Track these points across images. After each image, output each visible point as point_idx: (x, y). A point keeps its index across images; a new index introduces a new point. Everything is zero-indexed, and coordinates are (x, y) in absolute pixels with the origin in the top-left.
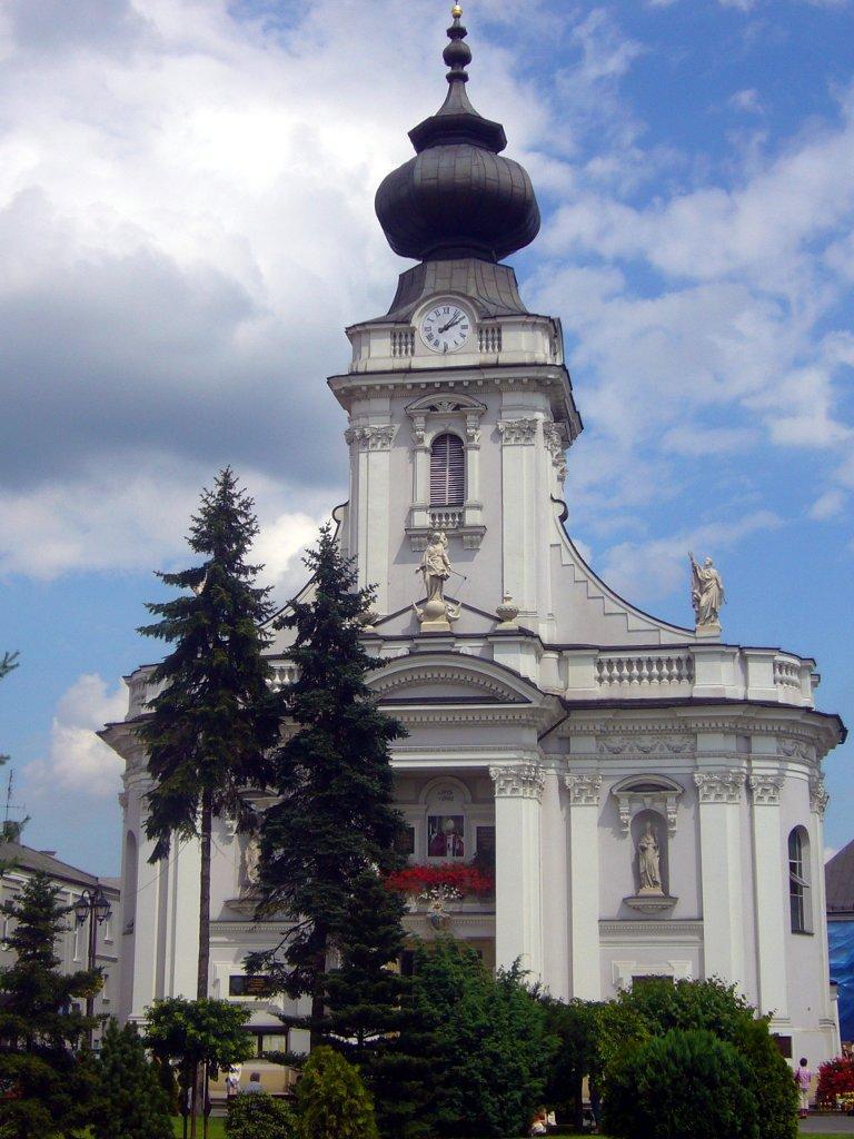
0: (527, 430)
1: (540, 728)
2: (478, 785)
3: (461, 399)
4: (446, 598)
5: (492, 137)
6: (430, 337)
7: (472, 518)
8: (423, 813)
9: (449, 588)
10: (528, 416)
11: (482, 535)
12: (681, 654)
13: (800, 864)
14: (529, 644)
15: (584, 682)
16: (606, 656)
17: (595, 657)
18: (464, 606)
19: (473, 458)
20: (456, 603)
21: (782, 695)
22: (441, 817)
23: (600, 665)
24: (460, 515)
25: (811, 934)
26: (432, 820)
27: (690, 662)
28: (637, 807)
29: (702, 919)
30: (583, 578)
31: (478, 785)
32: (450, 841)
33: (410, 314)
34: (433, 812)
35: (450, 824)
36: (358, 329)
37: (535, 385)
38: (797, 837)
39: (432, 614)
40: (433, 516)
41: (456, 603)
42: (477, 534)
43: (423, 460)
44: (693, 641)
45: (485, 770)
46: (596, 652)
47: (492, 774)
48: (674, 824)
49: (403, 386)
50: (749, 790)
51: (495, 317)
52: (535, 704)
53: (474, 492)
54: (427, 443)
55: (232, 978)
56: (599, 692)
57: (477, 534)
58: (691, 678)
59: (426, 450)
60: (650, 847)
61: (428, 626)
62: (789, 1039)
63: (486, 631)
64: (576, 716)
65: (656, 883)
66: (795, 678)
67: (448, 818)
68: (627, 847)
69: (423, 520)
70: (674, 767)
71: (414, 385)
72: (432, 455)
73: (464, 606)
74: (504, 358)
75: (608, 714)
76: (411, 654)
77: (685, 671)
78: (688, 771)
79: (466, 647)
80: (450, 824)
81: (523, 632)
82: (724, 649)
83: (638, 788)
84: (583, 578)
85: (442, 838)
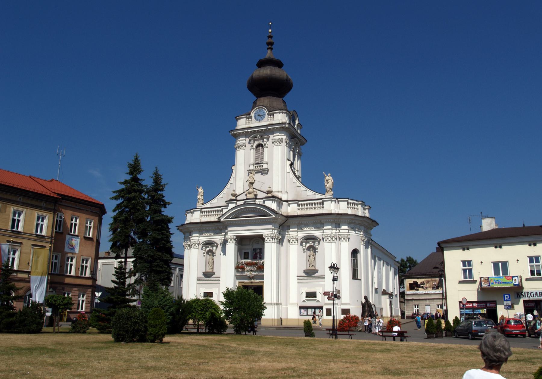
0: (280, 141)
1: (280, 223)
2: (260, 239)
3: (262, 134)
4: (254, 188)
5: (278, 64)
6: (255, 118)
7: (265, 166)
8: (251, 248)
9: (255, 186)
10: (280, 137)
11: (268, 171)
12: (321, 201)
13: (357, 260)
14: (275, 201)
15: (292, 210)
16: (300, 203)
17: (297, 203)
18: (258, 190)
19: (266, 150)
20: (256, 189)
21: (350, 212)
22: (256, 249)
23: (299, 205)
24: (263, 166)
25: (360, 280)
26: (254, 249)
27: (323, 204)
28: (308, 245)
29: (324, 276)
30: (296, 181)
31: (260, 239)
32: (258, 255)
33: (251, 113)
34: (254, 248)
35: (258, 251)
36: (238, 118)
37: (282, 129)
38: (355, 252)
39: (250, 193)
40: (256, 167)
41: (256, 189)
42: (266, 171)
43: (253, 152)
44: (324, 197)
45: (262, 235)
46: (297, 202)
47: (264, 236)
48: (317, 249)
49: (248, 132)
50: (340, 239)
51: (272, 111)
52: (274, 216)
53: (265, 160)
54: (254, 147)
55: (204, 293)
56: (300, 213)
57: (266, 171)
58: (323, 207)
59: (254, 149)
60: (311, 256)
61: (249, 196)
62: (350, 309)
63: (264, 197)
64: (291, 220)
65: (313, 266)
66: (355, 207)
67: (258, 249)
68: (304, 256)
69: (252, 167)
70: (318, 233)
71: (250, 131)
72: (256, 150)
73: (258, 190)
74: (274, 122)
75: (299, 219)
76: (244, 204)
77: (322, 206)
78: (321, 234)
79: (257, 202)
80: (258, 251)
81: (273, 197)
82: (331, 199)
83: (308, 239)
84: (296, 181)
85: (256, 254)
